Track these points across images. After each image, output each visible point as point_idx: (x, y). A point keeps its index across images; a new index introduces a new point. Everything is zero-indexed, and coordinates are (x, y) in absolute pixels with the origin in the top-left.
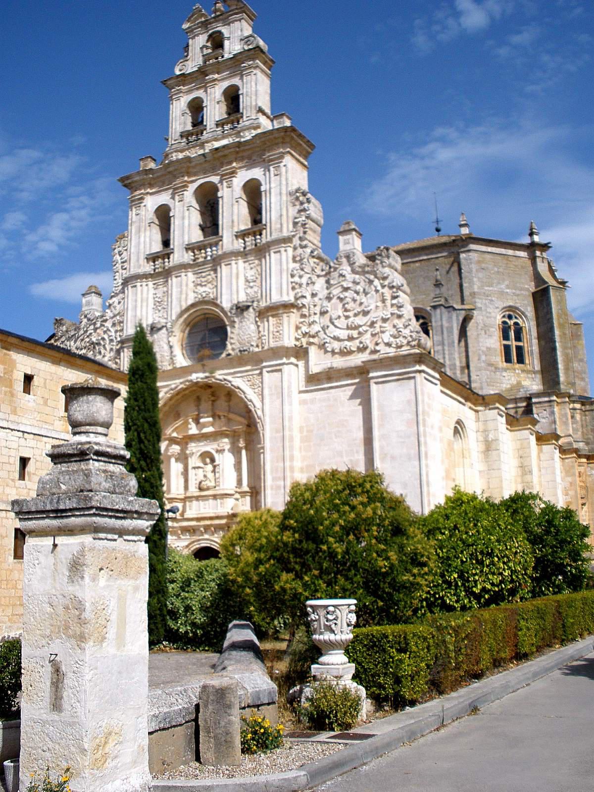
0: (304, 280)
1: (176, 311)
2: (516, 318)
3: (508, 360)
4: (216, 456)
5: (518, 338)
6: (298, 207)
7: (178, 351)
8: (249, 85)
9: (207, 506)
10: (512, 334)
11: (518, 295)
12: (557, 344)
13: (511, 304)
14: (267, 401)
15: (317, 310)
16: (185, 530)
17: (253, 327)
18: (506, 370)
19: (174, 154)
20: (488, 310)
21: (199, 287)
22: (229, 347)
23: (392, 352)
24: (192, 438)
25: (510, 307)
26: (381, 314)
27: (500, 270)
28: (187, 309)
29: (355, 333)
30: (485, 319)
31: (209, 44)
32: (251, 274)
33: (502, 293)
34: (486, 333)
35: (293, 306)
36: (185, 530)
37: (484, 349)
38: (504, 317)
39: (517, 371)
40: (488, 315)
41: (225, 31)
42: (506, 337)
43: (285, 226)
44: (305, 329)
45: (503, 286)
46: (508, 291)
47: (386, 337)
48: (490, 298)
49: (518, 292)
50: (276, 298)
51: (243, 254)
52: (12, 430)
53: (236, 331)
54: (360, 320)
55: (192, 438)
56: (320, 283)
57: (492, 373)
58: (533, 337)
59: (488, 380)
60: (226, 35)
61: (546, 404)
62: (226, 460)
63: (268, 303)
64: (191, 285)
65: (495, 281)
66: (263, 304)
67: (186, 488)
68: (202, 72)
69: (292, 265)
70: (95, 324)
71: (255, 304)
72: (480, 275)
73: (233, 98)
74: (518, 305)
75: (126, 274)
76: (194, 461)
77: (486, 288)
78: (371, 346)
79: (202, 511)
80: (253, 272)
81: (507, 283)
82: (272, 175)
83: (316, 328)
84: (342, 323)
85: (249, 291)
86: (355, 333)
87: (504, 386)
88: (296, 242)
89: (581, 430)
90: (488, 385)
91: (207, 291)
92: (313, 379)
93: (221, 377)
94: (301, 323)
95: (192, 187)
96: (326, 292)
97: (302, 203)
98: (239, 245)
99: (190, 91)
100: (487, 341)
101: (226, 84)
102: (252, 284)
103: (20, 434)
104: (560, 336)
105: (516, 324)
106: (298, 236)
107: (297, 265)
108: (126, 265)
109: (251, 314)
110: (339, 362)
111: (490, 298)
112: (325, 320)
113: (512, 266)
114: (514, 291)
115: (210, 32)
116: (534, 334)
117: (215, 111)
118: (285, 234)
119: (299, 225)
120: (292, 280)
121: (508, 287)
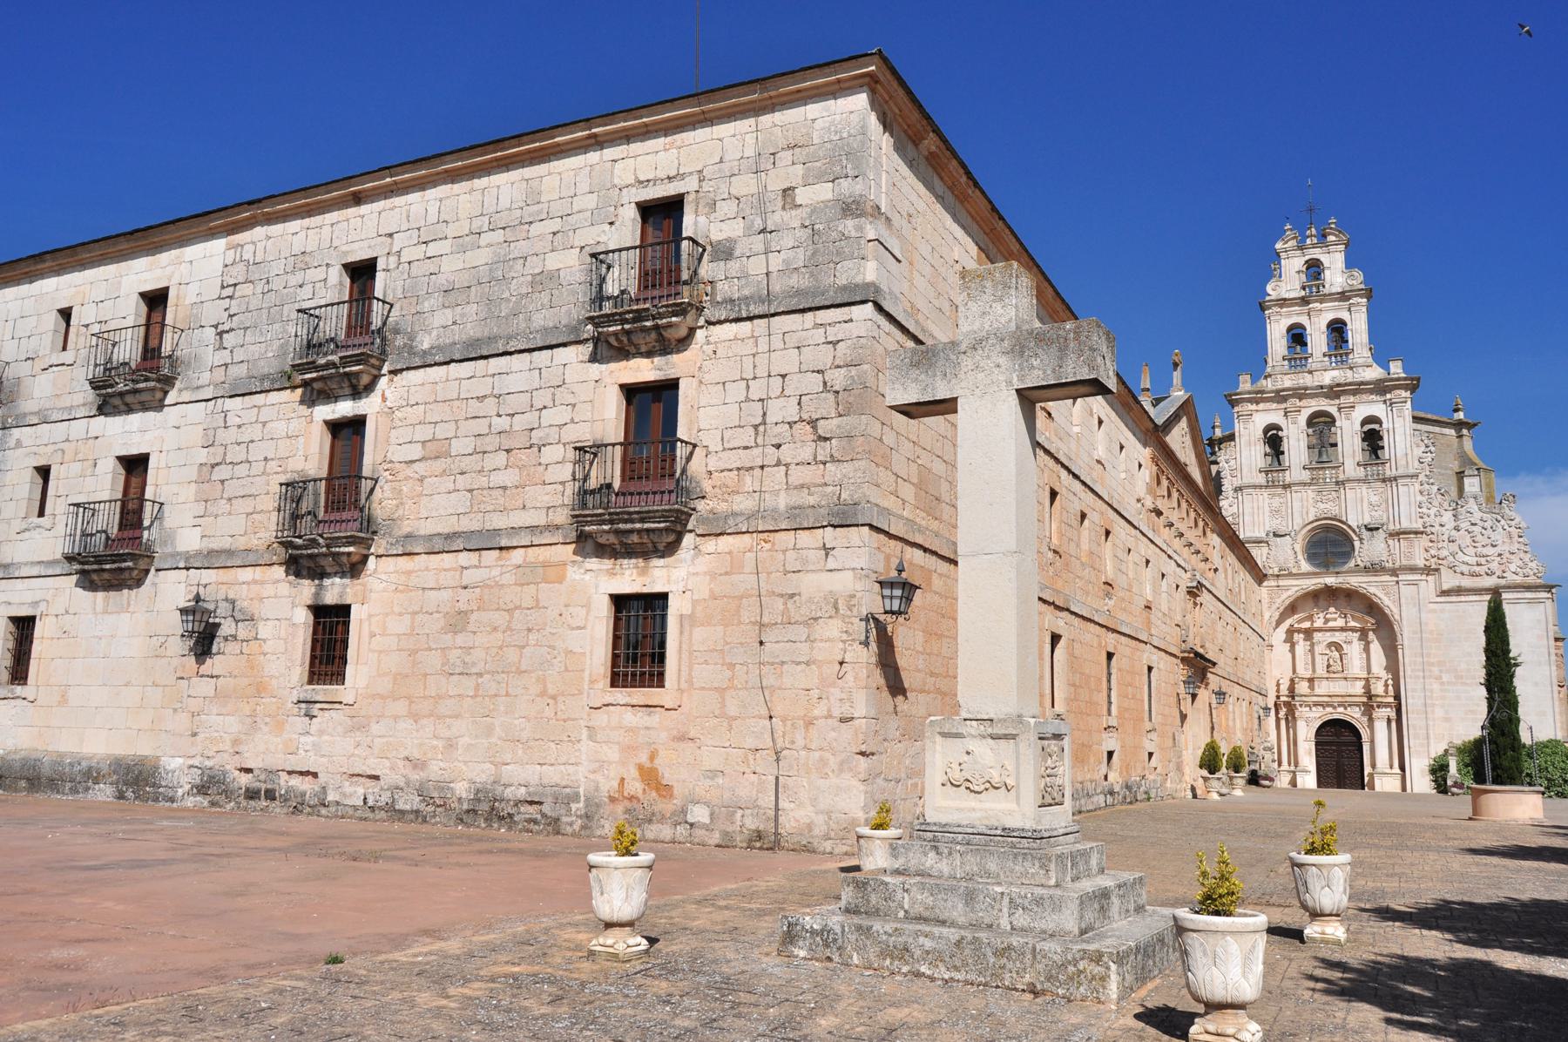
0: (1432, 512)
1: (1298, 522)
7: (1300, 557)
14: (1404, 608)
15: (1445, 537)
16: (1316, 704)
17: (1383, 545)
23: (1519, 579)
24: (1319, 630)
26: (1506, 548)
29: (1483, 561)
32: (1374, 499)
44: (1433, 552)
47: (1513, 567)
50: (1405, 525)
53: (1366, 546)
54: (1489, 551)
55: (1319, 630)
56: (1447, 516)
60: (1326, 264)
62: (1354, 649)
67: (1314, 670)
69: (1419, 498)
73: (1337, 330)
78: (1499, 573)
83: (1444, 553)
84: (1471, 551)
86: (1483, 561)
88: (1422, 477)
91: (1330, 508)
92: (1444, 593)
96: (1453, 524)
98: (1361, 472)
99: (1289, 315)
101: (1331, 316)
107: (1424, 499)
109: (1381, 534)
110: (1467, 582)
112: (1454, 547)
117: (1318, 341)
118: (1411, 471)
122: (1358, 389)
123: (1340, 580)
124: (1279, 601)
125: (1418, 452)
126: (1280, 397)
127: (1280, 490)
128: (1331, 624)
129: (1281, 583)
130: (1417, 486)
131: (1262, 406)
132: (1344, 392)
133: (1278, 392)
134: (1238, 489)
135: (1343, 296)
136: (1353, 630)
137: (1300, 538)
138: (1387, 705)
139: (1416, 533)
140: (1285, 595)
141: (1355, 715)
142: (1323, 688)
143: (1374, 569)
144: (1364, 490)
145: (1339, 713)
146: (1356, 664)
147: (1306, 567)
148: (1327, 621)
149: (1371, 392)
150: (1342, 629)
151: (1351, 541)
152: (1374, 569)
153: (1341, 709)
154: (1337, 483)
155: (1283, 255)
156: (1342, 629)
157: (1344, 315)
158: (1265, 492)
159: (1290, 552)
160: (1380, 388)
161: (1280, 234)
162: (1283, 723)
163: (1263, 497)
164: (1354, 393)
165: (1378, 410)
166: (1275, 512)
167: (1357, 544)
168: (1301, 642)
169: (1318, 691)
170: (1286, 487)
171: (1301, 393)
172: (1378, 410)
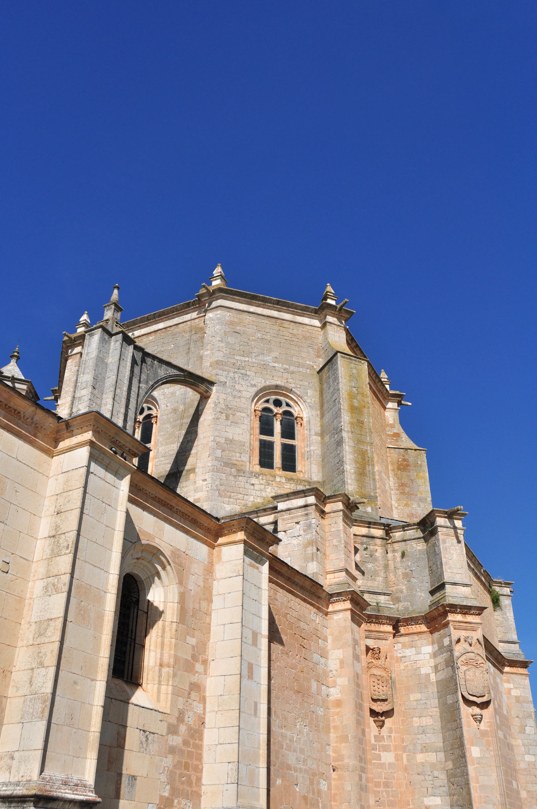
2: (288, 405)
3: (266, 460)
5: (289, 432)
10: (277, 427)
11: (293, 373)
12: (345, 434)
13: (279, 383)
18: (257, 475)
20: (238, 387)
25: (277, 387)
27: (264, 337)
30: (230, 398)
33: (264, 366)
34: (227, 418)
37: (223, 441)
38: (267, 401)
39: (278, 479)
40: (235, 393)
42: (266, 427)
45: (268, 358)
46: (276, 365)
48: (243, 371)
49: (292, 368)
57: (231, 478)
58: (313, 432)
59: (223, 488)
61: (301, 512)
65: (256, 350)
72: (231, 340)
74: (291, 386)
77: (238, 358)
81: (274, 355)
87: (252, 499)
89: (382, 574)
90: (220, 495)
100: (228, 429)
104: (352, 424)
105: (287, 413)
111: (243, 371)
113: (287, 334)
114: (285, 366)
116: (316, 427)
121: (276, 360)
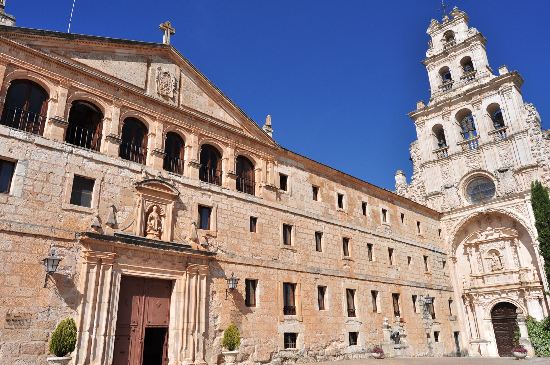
0: (542, 151)
4: (500, 251)
6: (528, 113)
7: (463, 198)
8: (477, 55)
9: (499, 279)
17: (512, 180)
19: (437, 98)
21: (470, 164)
22: (498, 192)
24: (482, 243)
28: (466, 175)
31: (444, 38)
32: (503, 153)
35: (537, 166)
36: (487, 293)
41: (454, 29)
43: (521, 125)
50: (524, 163)
51: (495, 143)
52: (403, 243)
53: (501, 183)
63: (520, 166)
64: (465, 163)
66: (516, 167)
68: (445, 53)
69: (531, 145)
70: (406, 189)
71: (511, 168)
73: (467, 63)
75: (422, 162)
76: (485, 255)
79: (496, 282)
80: (504, 152)
82: (506, 99)
85: (504, 161)
88: (530, 131)
93: (498, 208)
94: (545, 174)
95: (454, 113)
97: (530, 111)
98: (491, 138)
99: (439, 64)
101: (461, 57)
102: (505, 158)
103: (405, 245)
106: (531, 129)
107: (535, 144)
108: (420, 157)
109: (510, 173)
115: (444, 32)
117: (457, 72)
118: (523, 129)
119: (531, 122)
120: (533, 152)
122: (481, 90)
123: (487, 207)
124: (452, 228)
125: (525, 117)
126: (438, 108)
127: (446, 161)
128: (490, 238)
129: (452, 216)
130: (528, 138)
131: (429, 116)
132: (473, 95)
133: (435, 105)
134: (422, 166)
135: (466, 43)
136: (504, 239)
137: (460, 187)
138: (535, 289)
139: (532, 167)
140: (456, 223)
141: (513, 298)
142: (491, 281)
143: (509, 196)
144: (495, 149)
145: (504, 298)
146: (510, 263)
147: (467, 203)
148: (487, 236)
149: (490, 89)
150: (497, 240)
151: (492, 182)
152: (509, 196)
153: (504, 295)
154: (478, 148)
155: (432, 35)
156: (497, 240)
157: (469, 54)
158: (438, 165)
159: (456, 196)
160: (494, 86)
161: (428, 25)
162: (469, 308)
163: (437, 168)
164: (480, 93)
165: (496, 99)
166: (445, 175)
167: (496, 183)
168: (474, 253)
169: (488, 284)
170: (449, 158)
171: (449, 103)
172: (496, 99)
